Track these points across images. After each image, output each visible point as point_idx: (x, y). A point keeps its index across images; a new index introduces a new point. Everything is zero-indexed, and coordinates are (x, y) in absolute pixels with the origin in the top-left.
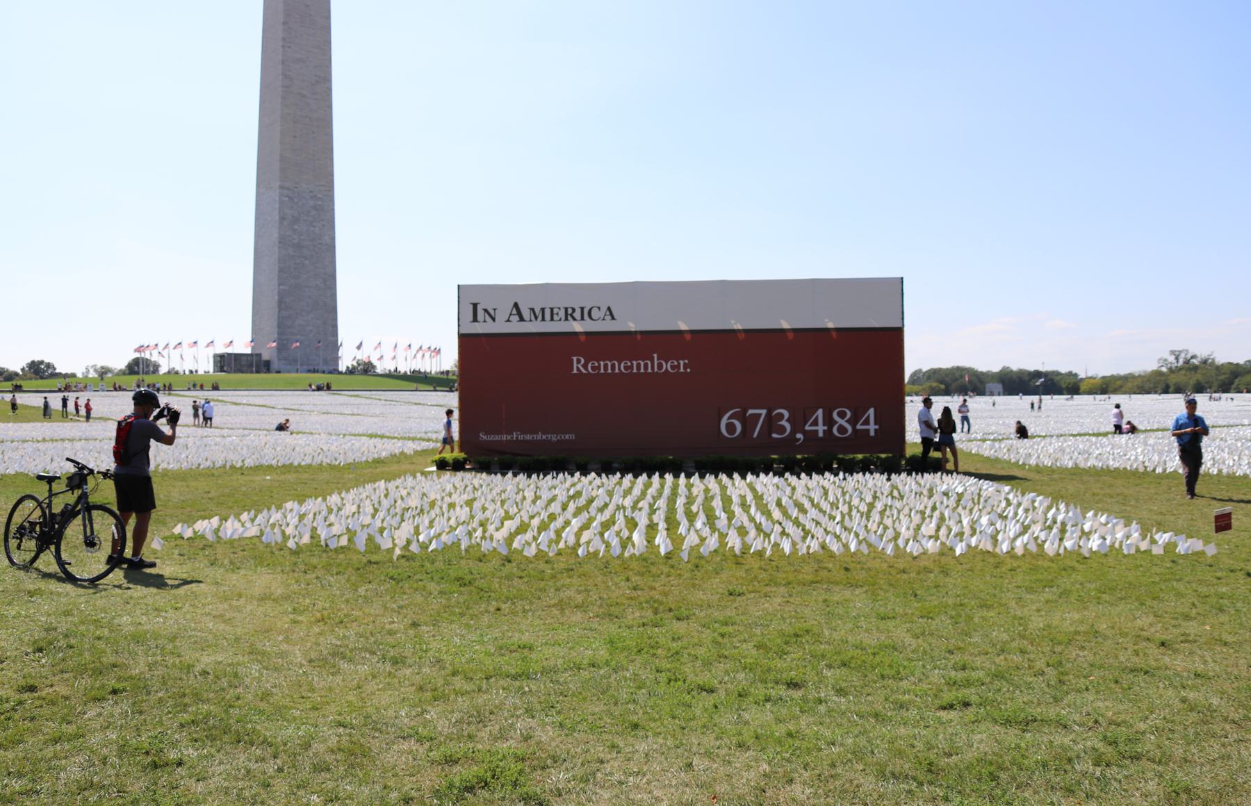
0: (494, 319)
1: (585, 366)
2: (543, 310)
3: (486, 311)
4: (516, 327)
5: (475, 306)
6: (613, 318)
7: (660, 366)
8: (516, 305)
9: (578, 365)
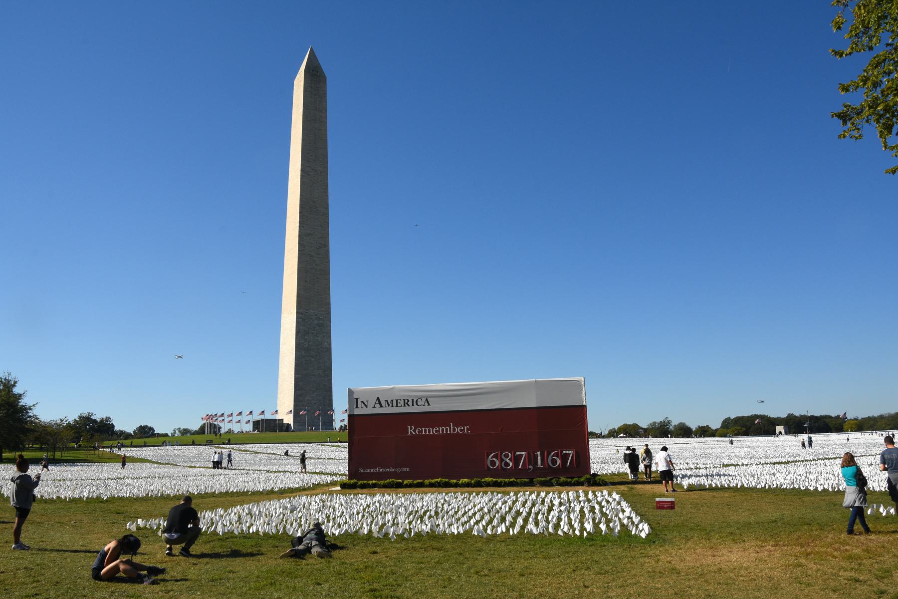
1: (414, 431)
4: (378, 410)
5: (357, 399)
7: (454, 430)
8: (378, 399)
9: (411, 430)
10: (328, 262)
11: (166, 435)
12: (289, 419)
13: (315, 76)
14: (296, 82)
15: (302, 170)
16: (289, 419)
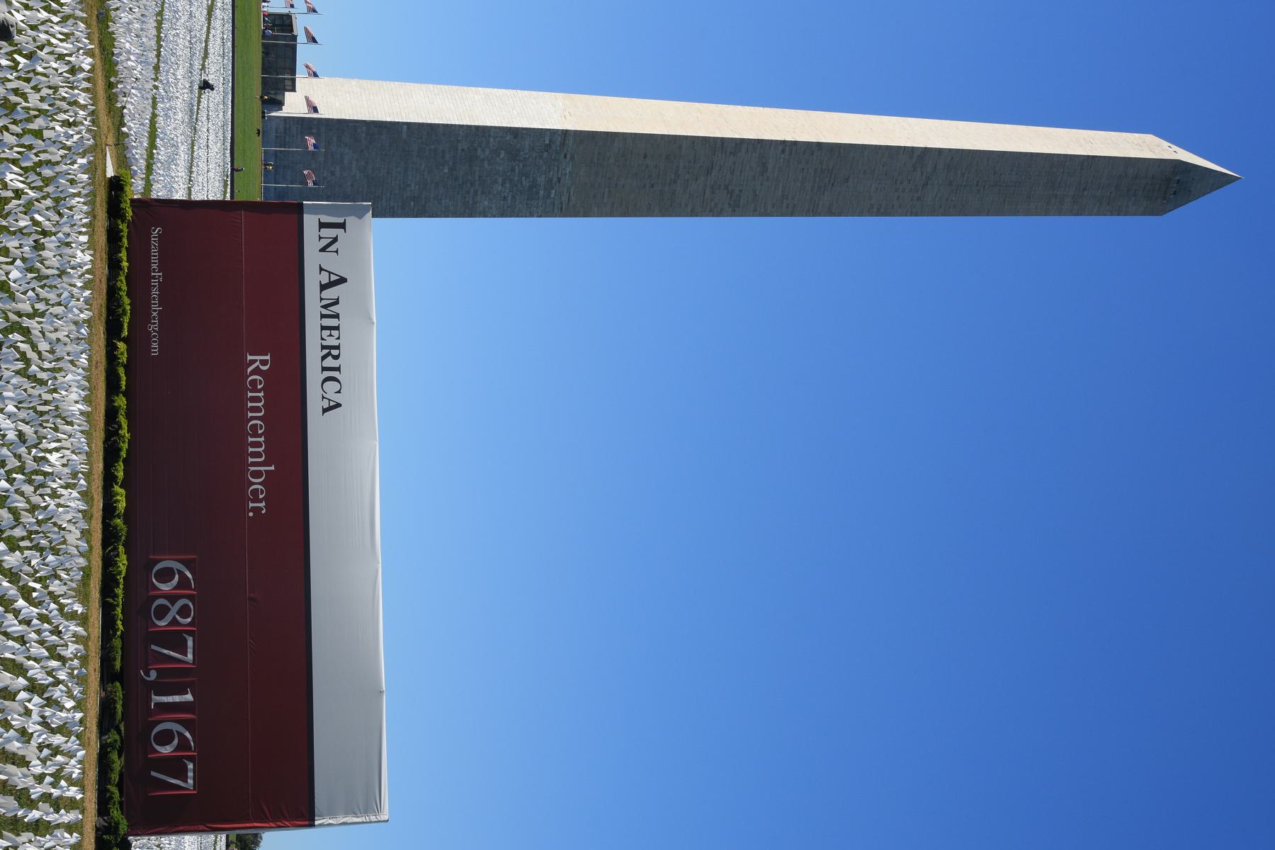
0: (323, 250)
2: (337, 316)
3: (335, 240)
5: (342, 226)
6: (325, 411)
7: (257, 474)
8: (342, 280)
9: (259, 361)
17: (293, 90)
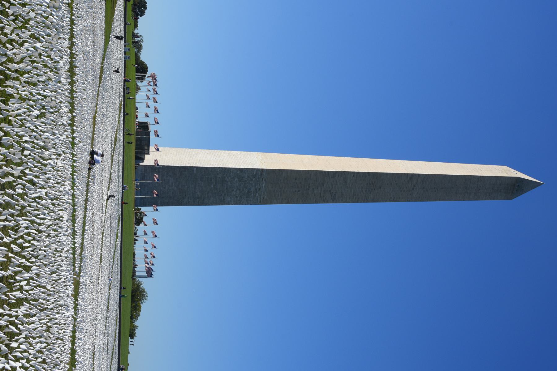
10: (316, 202)
11: (136, 26)
12: (149, 160)
13: (512, 188)
14: (505, 168)
15: (413, 175)
16: (149, 160)
17: (148, 153)
